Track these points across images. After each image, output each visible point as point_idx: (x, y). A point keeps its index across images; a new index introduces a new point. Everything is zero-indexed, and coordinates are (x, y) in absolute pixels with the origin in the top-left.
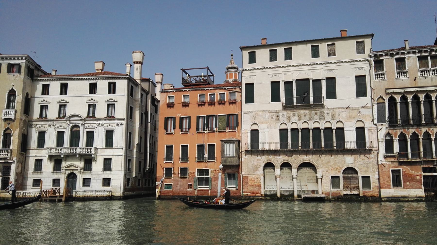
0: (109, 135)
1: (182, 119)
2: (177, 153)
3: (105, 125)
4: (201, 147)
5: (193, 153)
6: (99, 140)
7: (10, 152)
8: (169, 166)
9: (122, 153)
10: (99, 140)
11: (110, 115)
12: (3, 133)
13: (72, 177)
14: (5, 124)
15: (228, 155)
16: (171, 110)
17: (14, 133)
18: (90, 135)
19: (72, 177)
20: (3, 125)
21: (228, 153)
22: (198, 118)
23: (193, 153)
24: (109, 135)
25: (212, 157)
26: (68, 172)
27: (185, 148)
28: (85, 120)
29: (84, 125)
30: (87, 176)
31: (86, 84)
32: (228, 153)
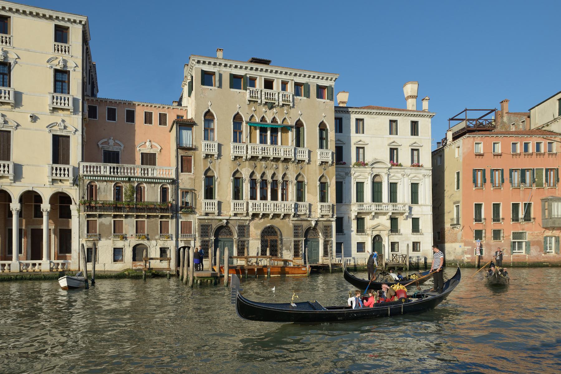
0: (415, 187)
1: (493, 171)
2: (486, 212)
3: (411, 176)
4: (515, 207)
5: (505, 212)
6: (404, 194)
7: (216, 204)
8: (479, 227)
9: (429, 211)
10: (404, 194)
11: (416, 162)
12: (318, 183)
13: (377, 241)
14: (320, 170)
15: (556, 217)
16: (479, 159)
17: (330, 182)
18: (393, 187)
19: (377, 241)
20: (318, 172)
21: (556, 214)
22: (511, 171)
23: (505, 212)
24: (415, 187)
25: (527, 218)
26: (375, 233)
27: (496, 207)
28: (389, 169)
29: (389, 175)
30: (395, 238)
31: (385, 120)
32: (556, 214)
